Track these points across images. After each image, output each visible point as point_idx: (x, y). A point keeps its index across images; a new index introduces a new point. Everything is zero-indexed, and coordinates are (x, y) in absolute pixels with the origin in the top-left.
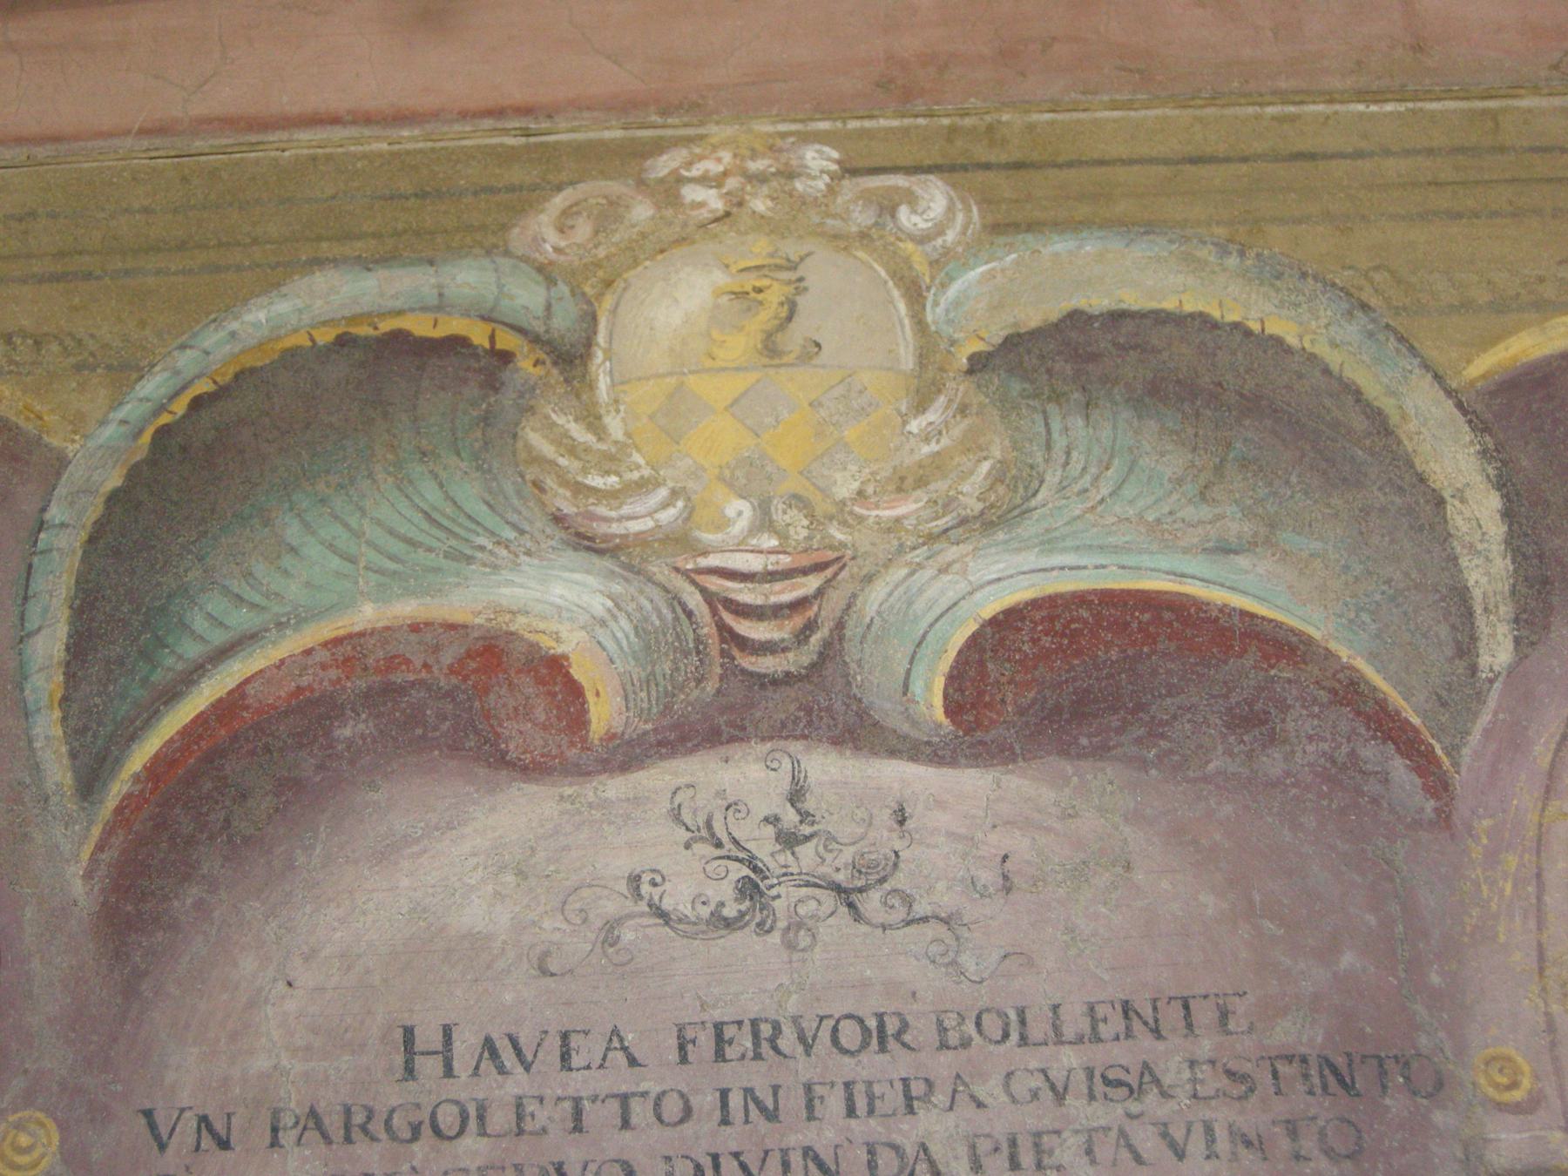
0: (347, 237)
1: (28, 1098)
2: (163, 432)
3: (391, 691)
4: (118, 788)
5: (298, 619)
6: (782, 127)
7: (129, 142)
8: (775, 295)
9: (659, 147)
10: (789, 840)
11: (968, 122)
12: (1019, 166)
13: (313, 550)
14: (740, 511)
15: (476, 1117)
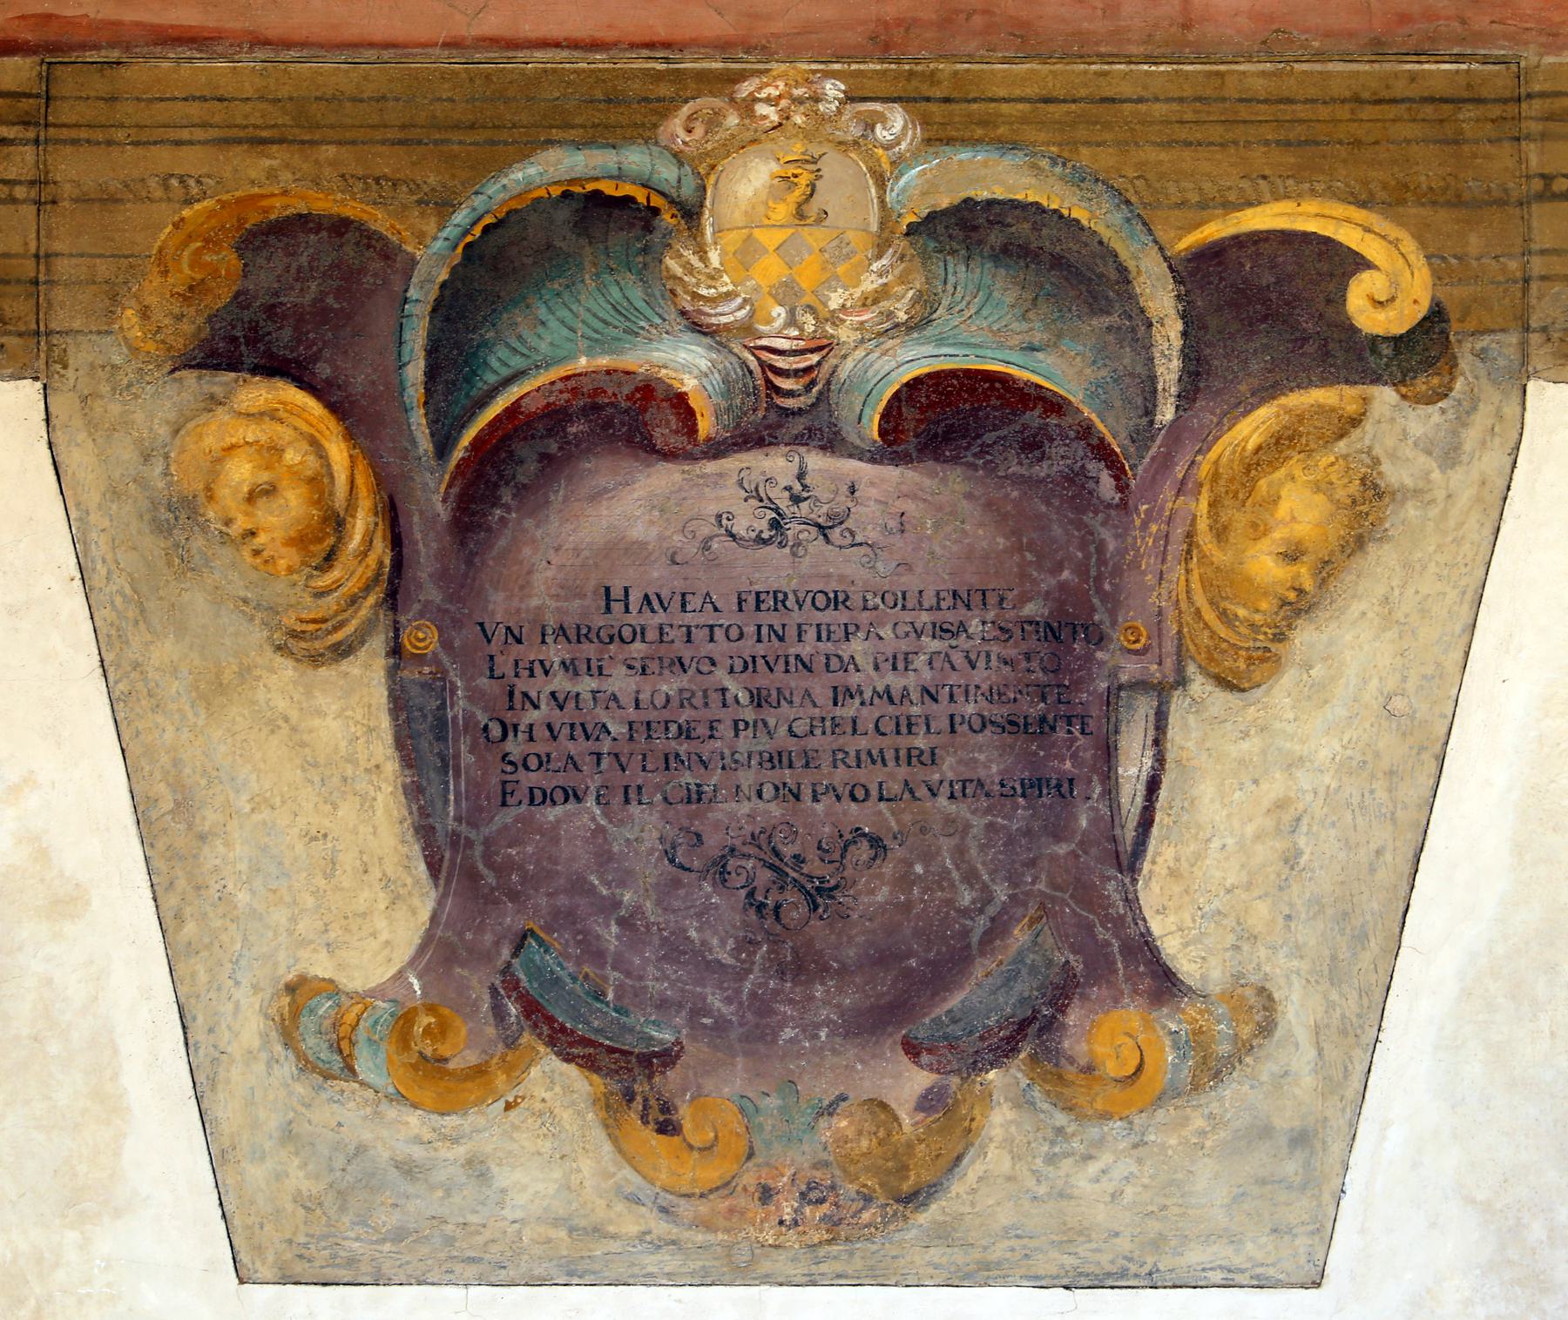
0: (568, 126)
1: (421, 615)
2: (468, 246)
3: (596, 408)
4: (458, 454)
5: (548, 364)
6: (814, 67)
7: (438, 51)
8: (804, 180)
9: (741, 76)
10: (796, 500)
11: (920, 68)
12: (947, 100)
13: (553, 324)
14: (779, 313)
15: (640, 633)
